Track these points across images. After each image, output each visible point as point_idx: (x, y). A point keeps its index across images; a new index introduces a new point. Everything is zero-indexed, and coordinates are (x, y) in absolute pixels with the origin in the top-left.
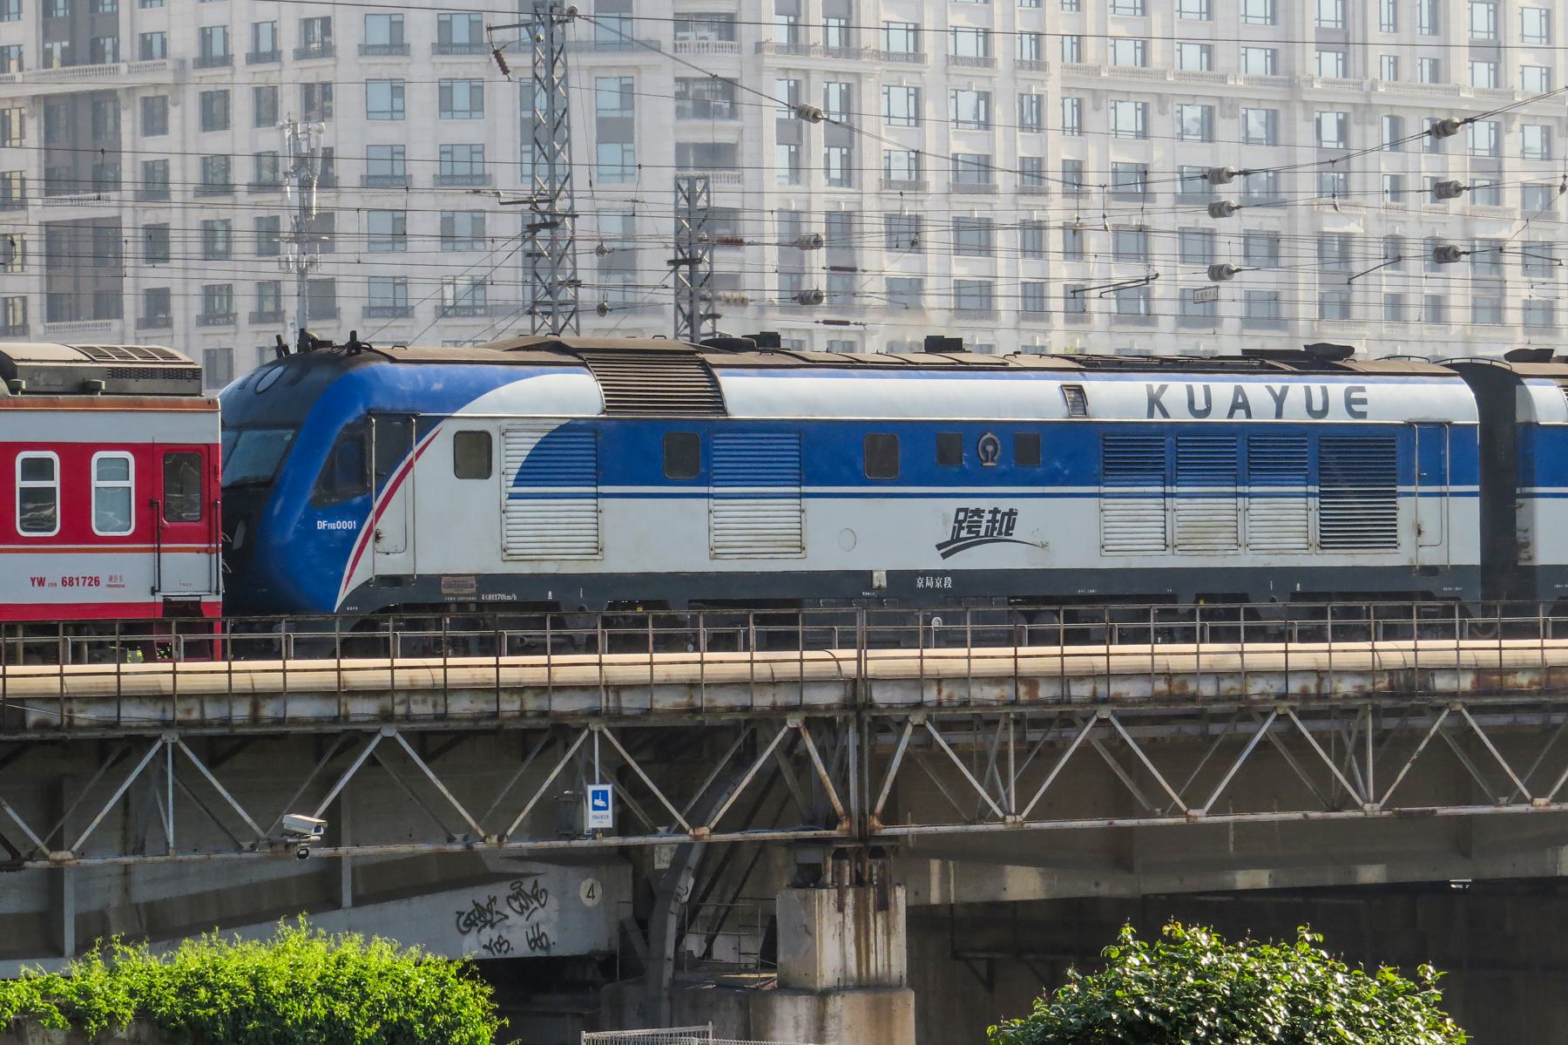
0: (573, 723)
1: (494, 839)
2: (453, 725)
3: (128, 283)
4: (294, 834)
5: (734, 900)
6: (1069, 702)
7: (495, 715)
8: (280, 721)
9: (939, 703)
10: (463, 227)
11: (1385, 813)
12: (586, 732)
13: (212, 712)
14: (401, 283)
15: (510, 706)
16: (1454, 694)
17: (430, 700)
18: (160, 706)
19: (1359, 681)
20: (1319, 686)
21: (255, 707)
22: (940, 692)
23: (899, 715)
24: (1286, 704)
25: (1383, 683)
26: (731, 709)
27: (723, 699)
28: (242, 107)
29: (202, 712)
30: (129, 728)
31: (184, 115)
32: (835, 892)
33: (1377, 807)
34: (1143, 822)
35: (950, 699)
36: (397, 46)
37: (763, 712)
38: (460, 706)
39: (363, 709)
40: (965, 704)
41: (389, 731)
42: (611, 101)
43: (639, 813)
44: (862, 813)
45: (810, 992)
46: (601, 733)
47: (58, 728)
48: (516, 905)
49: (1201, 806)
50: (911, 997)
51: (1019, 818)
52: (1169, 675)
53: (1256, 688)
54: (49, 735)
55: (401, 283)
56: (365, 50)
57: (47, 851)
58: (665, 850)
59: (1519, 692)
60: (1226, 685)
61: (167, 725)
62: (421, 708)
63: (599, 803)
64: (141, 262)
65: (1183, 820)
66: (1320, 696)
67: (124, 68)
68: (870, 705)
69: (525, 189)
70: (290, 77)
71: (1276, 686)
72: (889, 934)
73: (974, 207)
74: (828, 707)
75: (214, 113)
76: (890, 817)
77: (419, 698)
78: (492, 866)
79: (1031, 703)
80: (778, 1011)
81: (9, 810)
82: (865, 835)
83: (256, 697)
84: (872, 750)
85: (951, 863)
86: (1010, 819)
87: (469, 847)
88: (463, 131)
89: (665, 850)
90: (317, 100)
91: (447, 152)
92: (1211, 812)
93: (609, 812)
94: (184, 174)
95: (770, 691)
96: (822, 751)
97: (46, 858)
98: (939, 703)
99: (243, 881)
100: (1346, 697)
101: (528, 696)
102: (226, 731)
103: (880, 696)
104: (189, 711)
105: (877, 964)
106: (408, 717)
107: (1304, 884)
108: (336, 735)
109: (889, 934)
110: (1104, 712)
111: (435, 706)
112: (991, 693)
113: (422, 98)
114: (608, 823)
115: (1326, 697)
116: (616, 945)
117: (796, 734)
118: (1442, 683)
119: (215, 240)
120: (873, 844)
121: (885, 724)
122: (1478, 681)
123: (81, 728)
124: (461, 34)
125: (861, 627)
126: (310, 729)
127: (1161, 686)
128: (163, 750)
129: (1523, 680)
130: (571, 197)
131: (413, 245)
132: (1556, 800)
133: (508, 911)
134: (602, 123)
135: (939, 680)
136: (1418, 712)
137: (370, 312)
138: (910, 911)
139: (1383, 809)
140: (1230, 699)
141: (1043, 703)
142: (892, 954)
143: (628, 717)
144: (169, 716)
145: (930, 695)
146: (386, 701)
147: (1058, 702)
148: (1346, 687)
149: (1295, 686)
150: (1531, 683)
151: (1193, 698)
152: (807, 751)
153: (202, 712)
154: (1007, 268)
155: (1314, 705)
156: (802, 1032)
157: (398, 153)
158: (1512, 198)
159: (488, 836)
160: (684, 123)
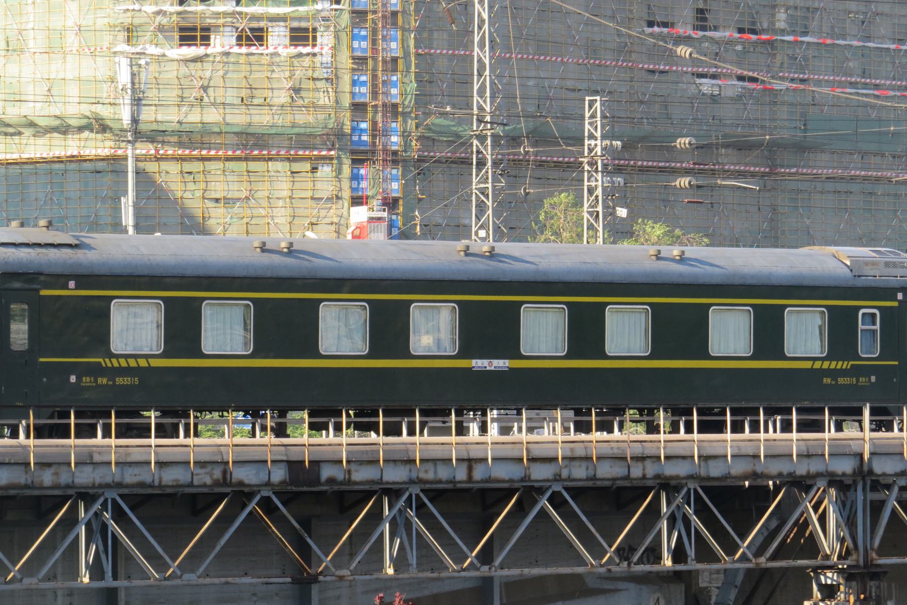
0: (673, 483)
2: (599, 483)
7: (627, 477)
8: (489, 480)
13: (443, 473)
15: (636, 472)
17: (584, 464)
18: (408, 467)
21: (470, 469)
23: (890, 481)
26: (780, 475)
29: (435, 472)
30: (387, 483)
37: (802, 477)
38: (606, 471)
39: (540, 473)
41: (557, 487)
44: (866, 550)
46: (695, 490)
47: (341, 483)
54: (336, 488)
58: (706, 574)
61: (411, 482)
62: (580, 472)
68: (871, 472)
74: (844, 474)
76: (881, 552)
77: (577, 463)
78: (591, 583)
82: (868, 564)
83: (470, 462)
84: (871, 502)
85: (893, 586)
87: (609, 570)
89: (706, 574)
95: (806, 461)
99: (426, 593)
101: (648, 463)
102: (450, 486)
103: (882, 467)
104: (426, 472)
106: (569, 479)
108: (516, 490)
111: (587, 469)
120: (873, 570)
121: (878, 484)
123: (356, 483)
126: (506, 485)
143: (714, 479)
144: (414, 475)
153: (435, 472)
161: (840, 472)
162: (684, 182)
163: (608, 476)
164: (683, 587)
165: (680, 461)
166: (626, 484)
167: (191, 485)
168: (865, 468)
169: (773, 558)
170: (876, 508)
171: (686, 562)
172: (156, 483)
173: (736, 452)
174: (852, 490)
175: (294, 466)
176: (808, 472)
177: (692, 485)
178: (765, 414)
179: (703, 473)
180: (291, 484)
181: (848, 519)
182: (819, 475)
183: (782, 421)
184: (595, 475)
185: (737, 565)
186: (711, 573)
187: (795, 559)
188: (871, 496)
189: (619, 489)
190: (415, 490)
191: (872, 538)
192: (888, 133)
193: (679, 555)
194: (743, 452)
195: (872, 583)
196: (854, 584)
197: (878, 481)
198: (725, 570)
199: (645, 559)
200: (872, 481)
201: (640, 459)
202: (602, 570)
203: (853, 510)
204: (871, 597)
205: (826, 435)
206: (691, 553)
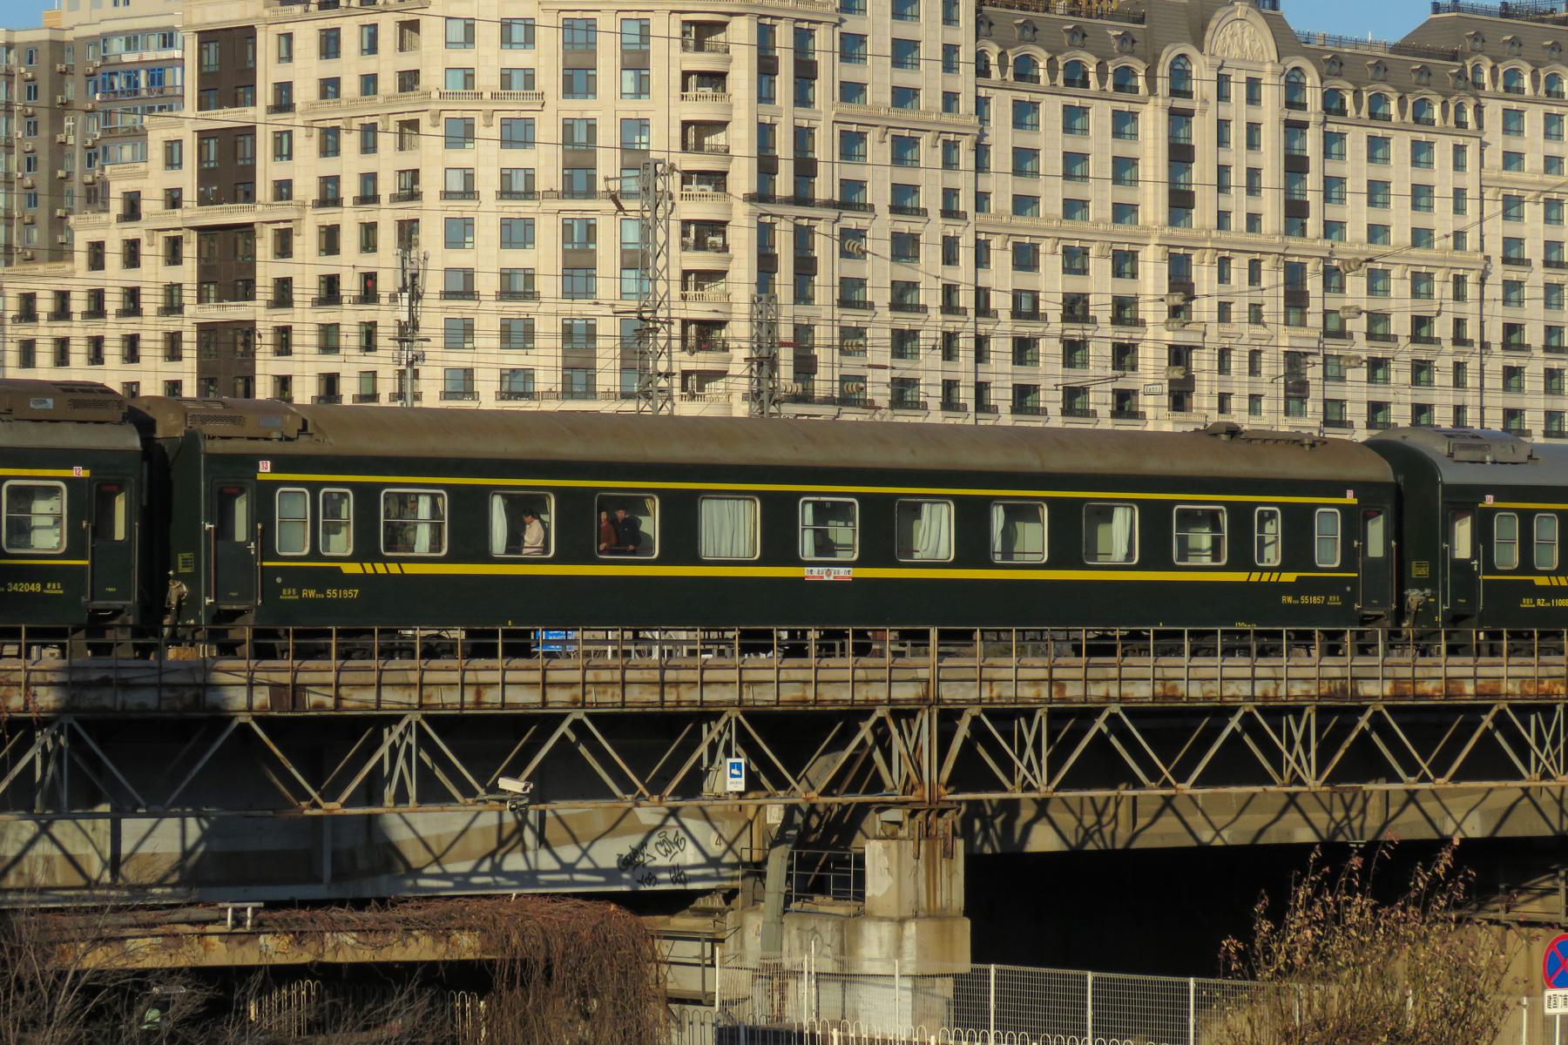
3: (259, 368)
4: (504, 791)
10: (518, 328)
12: (724, 720)
14: (472, 370)
15: (671, 696)
17: (610, 691)
19: (1305, 687)
20: (1276, 689)
21: (478, 694)
26: (835, 701)
27: (828, 693)
28: (350, 239)
31: (306, 242)
32: (911, 844)
35: (999, 697)
36: (469, 193)
38: (634, 694)
39: (558, 697)
41: (579, 714)
42: (632, 234)
43: (764, 780)
45: (891, 920)
46: (737, 720)
48: (662, 849)
50: (967, 923)
53: (1231, 690)
55: (468, 373)
56: (447, 195)
57: (320, 801)
59: (1426, 696)
60: (1208, 687)
63: (735, 772)
64: (269, 356)
67: (259, 207)
68: (939, 700)
69: (633, 304)
70: (387, 217)
71: (1245, 689)
72: (950, 876)
73: (905, 321)
75: (330, 240)
77: (600, 689)
80: (866, 933)
81: (293, 771)
83: (480, 687)
86: (1043, 789)
88: (517, 259)
90: (408, 232)
91: (506, 275)
93: (743, 779)
94: (306, 285)
96: (901, 733)
97: (319, 806)
101: (683, 688)
103: (949, 693)
104: (429, 697)
105: (942, 898)
109: (950, 876)
110: (1115, 708)
112: (1028, 692)
113: (487, 229)
114: (742, 788)
117: (881, 722)
118: (1368, 689)
119: (329, 339)
120: (942, 806)
124: (519, 186)
127: (1159, 689)
128: (409, 725)
129: (1428, 687)
130: (669, 309)
131: (478, 342)
133: (656, 854)
134: (623, 252)
135: (991, 681)
137: (446, 395)
140: (1207, 699)
141: (1069, 700)
142: (953, 890)
145: (986, 694)
146: (578, 691)
148: (1298, 689)
149: (1258, 692)
150: (1435, 690)
152: (888, 733)
154: (928, 369)
156: (885, 949)
157: (468, 275)
158: (1314, 320)
159: (652, 793)
160: (685, 254)
165: (719, 687)
167: (158, 710)
172: (118, 707)
175: (275, 687)
180: (272, 709)
182: (878, 702)
184: (623, 702)
190: (416, 716)
195: (940, 821)
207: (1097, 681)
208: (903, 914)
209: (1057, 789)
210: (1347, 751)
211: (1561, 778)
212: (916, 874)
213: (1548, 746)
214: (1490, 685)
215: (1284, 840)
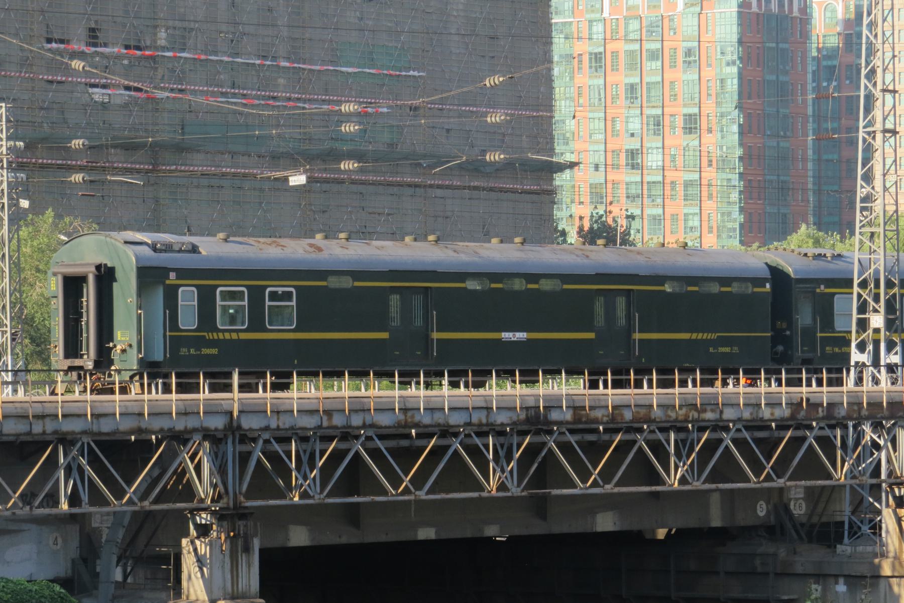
0: (69, 437)
1: (28, 508)
5: (146, 546)
6: (350, 427)
7: (29, 433)
9: (278, 426)
11: (523, 494)
12: (79, 444)
15: (37, 428)
16: (559, 423)
20: (487, 416)
22: (278, 419)
24: (469, 428)
25: (523, 416)
33: (519, 489)
34: (391, 498)
37: (180, 432)
40: (292, 428)
44: (235, 493)
46: (88, 444)
49: (419, 487)
51: (322, 496)
52: (404, 410)
58: (98, 516)
59: (596, 421)
65: (412, 497)
66: (487, 425)
68: (239, 427)
72: (249, 566)
74: (216, 430)
76: (249, 496)
79: (328, 428)
82: (237, 506)
84: (240, 453)
85: (259, 524)
86: (317, 497)
87: (14, 514)
92: (428, 493)
95: (184, 417)
98: (278, 426)
100: (502, 424)
101: (47, 420)
103: (250, 423)
105: (242, 584)
107: (404, 539)
109: (249, 566)
110: (370, 433)
115: (492, 424)
116: (70, 572)
118: (555, 416)
120: (241, 511)
121: (246, 438)
122: (574, 414)
125: (236, 379)
127: (402, 417)
129: (598, 414)
132: (617, 485)
136: (538, 432)
138: (262, 551)
139: (523, 491)
140: (439, 425)
141: (336, 427)
142: (251, 577)
147: (344, 427)
149: (475, 420)
150: (603, 416)
151: (416, 425)
155: (485, 429)
161: (213, 428)
162: (78, 177)
163: (13, 432)
164: (77, 528)
165: (75, 420)
166: (29, 439)
168: (235, 424)
169: (156, 501)
170: (244, 458)
171: (80, 506)
173: (124, 410)
174: (224, 442)
176: (186, 427)
177: (86, 439)
178: (148, 378)
179: (95, 429)
181: (220, 467)
182: (195, 430)
183: (164, 384)
185: (125, 508)
186: (102, 516)
187: (174, 502)
188: (239, 448)
189: (24, 444)
191: (240, 484)
192: (254, 136)
193: (74, 499)
194: (130, 411)
195: (240, 523)
196: (225, 523)
197: (245, 435)
198: (115, 513)
199: (45, 504)
200: (240, 435)
201: (41, 417)
202: (8, 513)
203: (224, 461)
204: (239, 534)
205: (201, 396)
206: (85, 497)
207: (356, 411)
208: (214, 597)
209: (328, 496)
210: (540, 464)
211: (695, 483)
212: (223, 567)
213: (684, 458)
214: (643, 411)
215: (478, 535)
